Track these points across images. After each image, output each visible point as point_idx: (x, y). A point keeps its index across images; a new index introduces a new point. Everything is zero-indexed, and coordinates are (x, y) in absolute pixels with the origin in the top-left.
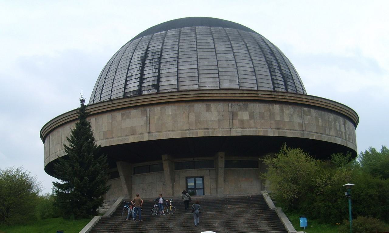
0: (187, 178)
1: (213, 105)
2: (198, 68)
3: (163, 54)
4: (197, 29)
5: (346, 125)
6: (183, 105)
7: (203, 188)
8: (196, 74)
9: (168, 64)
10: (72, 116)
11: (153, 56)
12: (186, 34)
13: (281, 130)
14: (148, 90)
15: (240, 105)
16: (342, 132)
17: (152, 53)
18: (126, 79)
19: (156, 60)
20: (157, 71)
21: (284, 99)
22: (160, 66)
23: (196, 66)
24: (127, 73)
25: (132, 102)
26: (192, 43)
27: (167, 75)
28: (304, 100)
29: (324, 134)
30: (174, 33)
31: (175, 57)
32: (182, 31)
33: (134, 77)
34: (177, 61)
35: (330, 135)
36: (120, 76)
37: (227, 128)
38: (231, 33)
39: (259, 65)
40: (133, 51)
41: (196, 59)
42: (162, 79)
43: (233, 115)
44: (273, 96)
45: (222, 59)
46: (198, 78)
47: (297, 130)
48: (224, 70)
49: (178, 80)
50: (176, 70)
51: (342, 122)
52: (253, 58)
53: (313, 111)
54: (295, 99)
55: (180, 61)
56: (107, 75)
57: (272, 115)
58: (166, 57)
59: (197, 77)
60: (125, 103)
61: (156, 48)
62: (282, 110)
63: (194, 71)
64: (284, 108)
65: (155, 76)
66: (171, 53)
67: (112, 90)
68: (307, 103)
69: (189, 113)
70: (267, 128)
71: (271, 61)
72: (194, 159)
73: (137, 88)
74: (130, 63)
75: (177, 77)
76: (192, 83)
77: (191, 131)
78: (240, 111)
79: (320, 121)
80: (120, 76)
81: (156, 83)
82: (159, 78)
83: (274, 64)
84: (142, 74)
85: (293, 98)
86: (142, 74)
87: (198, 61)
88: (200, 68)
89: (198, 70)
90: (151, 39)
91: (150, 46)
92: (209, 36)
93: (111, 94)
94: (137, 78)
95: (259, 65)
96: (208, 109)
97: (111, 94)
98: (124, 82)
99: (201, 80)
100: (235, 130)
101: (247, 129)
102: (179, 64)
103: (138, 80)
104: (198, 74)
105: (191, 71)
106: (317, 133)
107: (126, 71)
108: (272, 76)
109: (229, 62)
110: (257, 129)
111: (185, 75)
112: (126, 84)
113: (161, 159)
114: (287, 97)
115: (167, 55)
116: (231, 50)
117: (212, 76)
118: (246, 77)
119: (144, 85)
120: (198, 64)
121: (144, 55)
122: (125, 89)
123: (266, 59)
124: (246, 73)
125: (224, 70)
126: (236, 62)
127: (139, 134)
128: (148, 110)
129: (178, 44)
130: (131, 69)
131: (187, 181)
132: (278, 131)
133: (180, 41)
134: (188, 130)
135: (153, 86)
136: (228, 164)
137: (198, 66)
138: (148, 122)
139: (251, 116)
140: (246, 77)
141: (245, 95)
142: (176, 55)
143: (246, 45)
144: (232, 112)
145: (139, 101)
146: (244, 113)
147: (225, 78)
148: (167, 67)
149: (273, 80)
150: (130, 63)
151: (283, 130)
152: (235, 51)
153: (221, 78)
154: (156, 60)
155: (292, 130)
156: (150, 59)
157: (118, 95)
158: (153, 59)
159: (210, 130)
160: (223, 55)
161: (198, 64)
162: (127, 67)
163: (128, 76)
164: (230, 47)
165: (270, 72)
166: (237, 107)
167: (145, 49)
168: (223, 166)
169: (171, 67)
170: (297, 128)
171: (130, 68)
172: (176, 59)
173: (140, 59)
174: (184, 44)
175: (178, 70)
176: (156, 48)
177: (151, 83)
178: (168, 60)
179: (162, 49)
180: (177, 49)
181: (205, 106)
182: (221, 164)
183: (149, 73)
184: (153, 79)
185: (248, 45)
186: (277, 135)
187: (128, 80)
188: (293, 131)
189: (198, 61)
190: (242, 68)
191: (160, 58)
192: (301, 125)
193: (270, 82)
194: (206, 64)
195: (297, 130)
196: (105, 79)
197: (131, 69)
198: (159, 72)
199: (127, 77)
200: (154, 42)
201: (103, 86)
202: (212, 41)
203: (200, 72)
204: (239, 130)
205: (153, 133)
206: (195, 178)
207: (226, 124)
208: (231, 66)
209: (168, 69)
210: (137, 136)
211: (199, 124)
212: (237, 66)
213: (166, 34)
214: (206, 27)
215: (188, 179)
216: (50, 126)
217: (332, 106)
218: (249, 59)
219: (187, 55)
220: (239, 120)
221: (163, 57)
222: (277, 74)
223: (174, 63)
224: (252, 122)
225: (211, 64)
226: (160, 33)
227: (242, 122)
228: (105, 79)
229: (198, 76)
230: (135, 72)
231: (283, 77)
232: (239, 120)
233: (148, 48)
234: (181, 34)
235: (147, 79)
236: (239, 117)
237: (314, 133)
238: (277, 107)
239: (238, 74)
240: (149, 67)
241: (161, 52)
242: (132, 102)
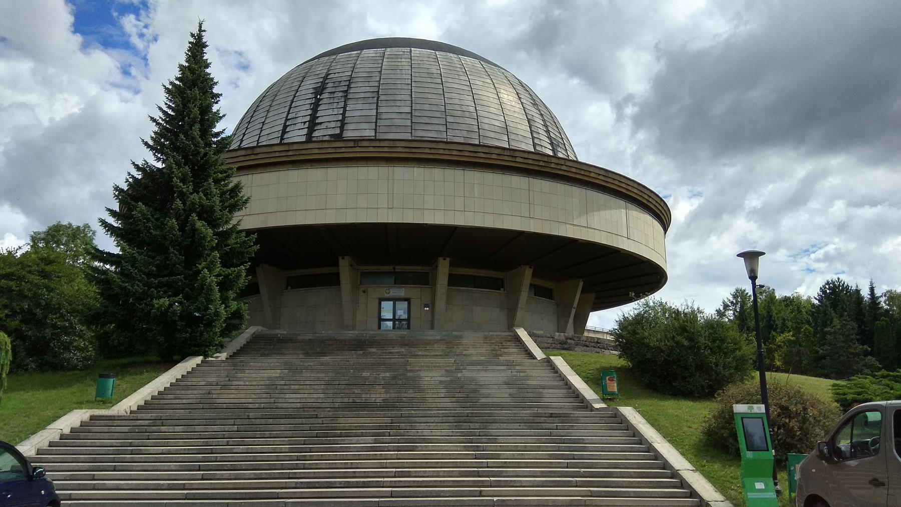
0: (381, 300)
8: (409, 123)
18: (285, 123)
19: (341, 94)
21: (560, 169)
22: (346, 105)
24: (288, 113)
33: (300, 120)
40: (301, 79)
42: (346, 127)
49: (375, 130)
55: (382, 98)
56: (252, 117)
60: (277, 154)
61: (341, 75)
63: (404, 116)
68: (597, 181)
73: (303, 139)
81: (338, 131)
82: (343, 124)
84: (314, 117)
85: (574, 170)
86: (314, 117)
94: (305, 123)
98: (281, 127)
103: (307, 125)
105: (400, 116)
108: (533, 138)
109: (464, 108)
112: (284, 132)
113: (336, 264)
114: (564, 168)
119: (315, 134)
129: (380, 72)
131: (380, 304)
136: (454, 280)
140: (492, 135)
141: (494, 156)
145: (303, 152)
154: (341, 94)
168: (446, 283)
172: (375, 95)
173: (312, 91)
176: (341, 75)
183: (328, 115)
196: (249, 122)
199: (287, 120)
201: (244, 135)
223: (370, 100)
228: (249, 122)
230: (303, 112)
231: (552, 144)
242: (291, 153)
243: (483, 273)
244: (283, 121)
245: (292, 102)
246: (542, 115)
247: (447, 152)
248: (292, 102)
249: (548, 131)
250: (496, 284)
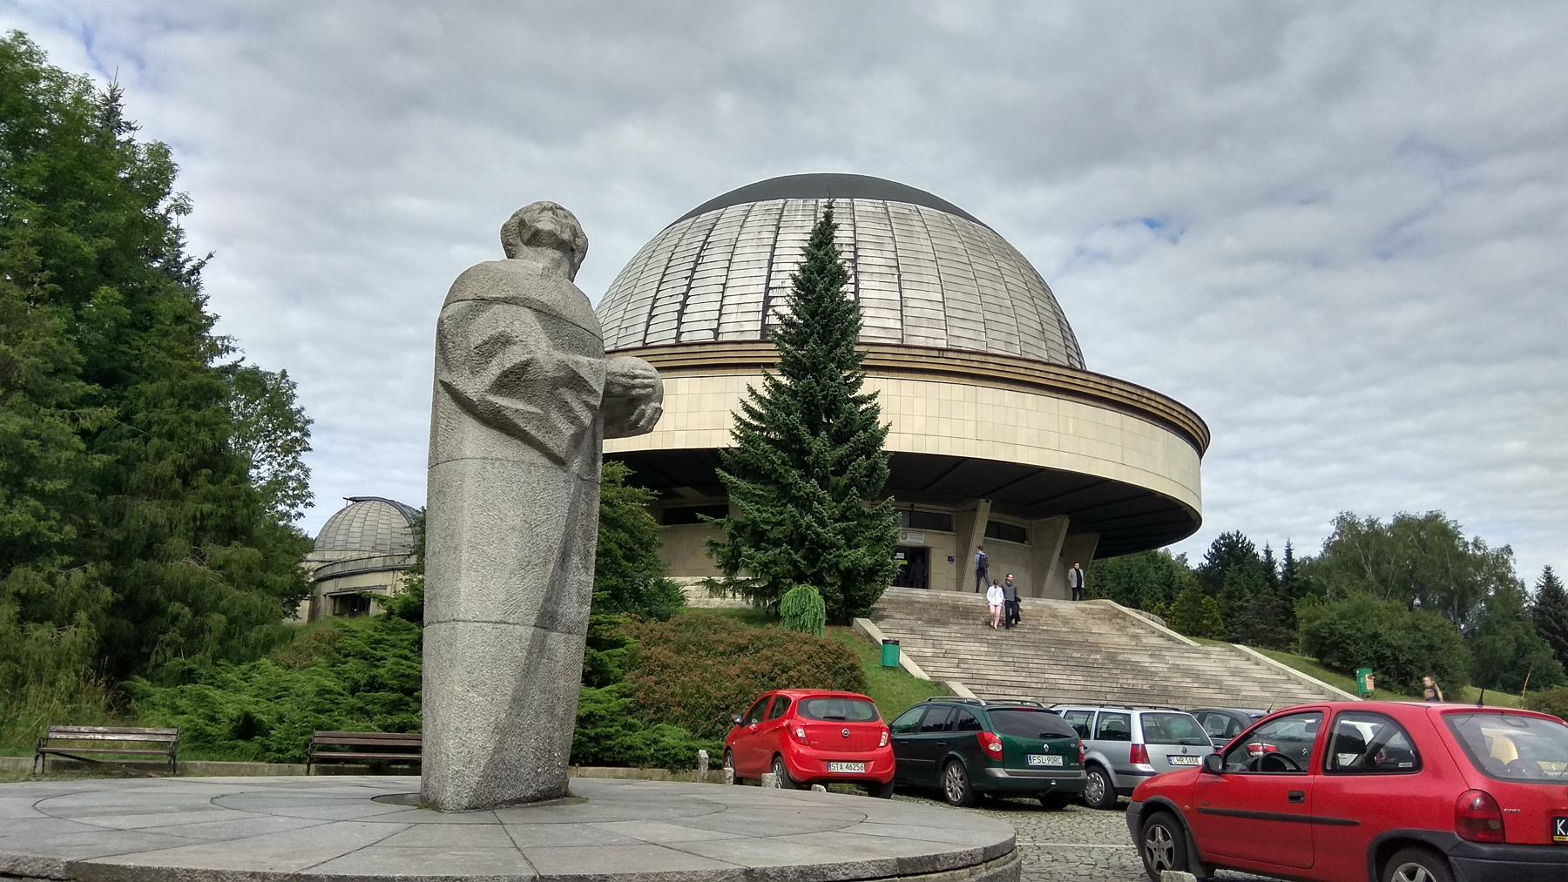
18: (766, 293)
24: (769, 279)
58: (869, 260)
98: (761, 298)
105: (928, 305)
107: (765, 272)
109: (1001, 302)
136: (994, 530)
150: (772, 255)
160: (988, 283)
171: (774, 268)
178: (876, 269)
182: (980, 528)
194: (959, 296)
199: (768, 289)
223: (889, 278)
244: (762, 288)
245: (771, 263)
248: (771, 263)
250: (1020, 536)
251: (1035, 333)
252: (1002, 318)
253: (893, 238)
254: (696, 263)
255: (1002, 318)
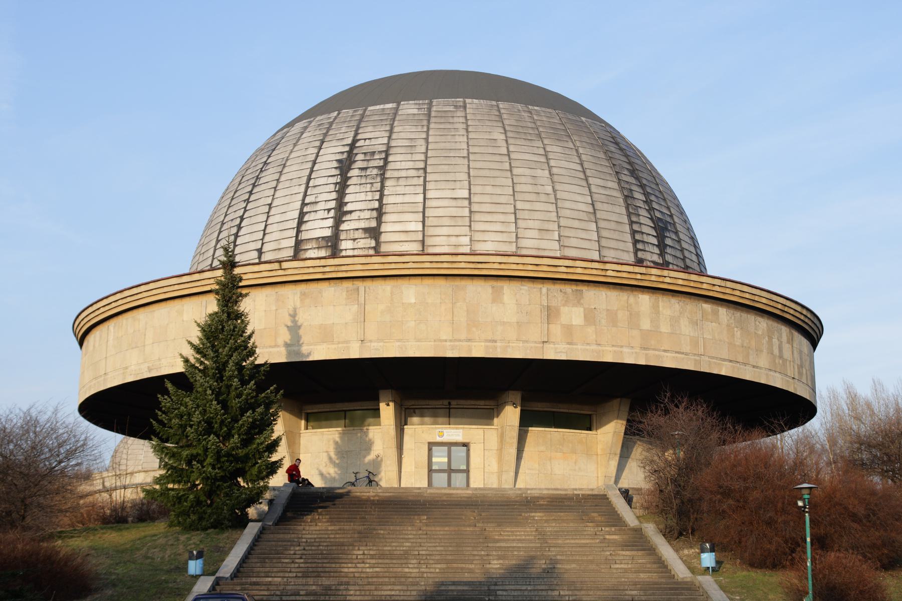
1: (508, 288)
2: (470, 199)
3: (390, 159)
4: (468, 106)
5: (795, 345)
6: (441, 282)
7: (467, 471)
8: (466, 212)
9: (402, 182)
10: (177, 287)
11: (368, 160)
12: (443, 115)
13: (651, 352)
14: (354, 240)
15: (565, 293)
16: (785, 361)
17: (365, 154)
18: (302, 209)
19: (375, 171)
20: (377, 197)
23: (465, 194)
24: (305, 195)
25: (327, 269)
26: (458, 139)
27: (400, 208)
28: (705, 286)
29: (745, 364)
30: (416, 111)
31: (418, 169)
32: (434, 109)
33: (321, 206)
34: (422, 179)
35: (757, 367)
36: (287, 200)
37: (536, 342)
38: (544, 119)
39: (603, 198)
40: (318, 144)
41: (465, 177)
42: (385, 218)
43: (550, 314)
44: (639, 277)
45: (523, 180)
46: (471, 221)
47: (686, 354)
48: (527, 206)
49: (423, 222)
50: (420, 198)
51: (784, 338)
52: (591, 180)
53: (723, 311)
54: (685, 283)
57: (634, 318)
58: (398, 166)
59: (467, 219)
60: (311, 270)
62: (655, 308)
64: (661, 304)
65: (373, 210)
66: (409, 157)
67: (264, 230)
69: (453, 304)
70: (622, 347)
71: (631, 190)
72: (450, 404)
73: (328, 233)
74: (312, 171)
75: (421, 215)
76: (457, 231)
77: (457, 343)
78: (564, 305)
79: (738, 333)
80: (287, 200)
81: (374, 224)
82: (380, 212)
83: (636, 195)
84: (340, 202)
85: (680, 282)
86: (340, 202)
87: (470, 182)
88: (474, 199)
89: (470, 203)
90: (360, 121)
91: (359, 137)
92: (495, 124)
93: (262, 239)
94: (329, 210)
95: (603, 198)
96: (497, 298)
97: (262, 239)
98: (296, 214)
99: (476, 226)
100: (552, 346)
101: (579, 347)
102: (428, 186)
103: (332, 213)
104: (471, 212)
105: (453, 203)
106: (731, 361)
107: (303, 187)
109: (540, 189)
110: (600, 348)
111: (440, 212)
112: (301, 222)
114: (667, 280)
115: (398, 161)
116: (543, 159)
117: (501, 218)
118: (576, 224)
119: (344, 227)
120: (470, 190)
121: (345, 156)
122: (299, 231)
123: (619, 184)
124: (575, 215)
125: (527, 206)
126: (555, 191)
127: (339, 343)
128: (362, 290)
129: (427, 140)
130: (315, 187)
132: (646, 355)
133: (431, 133)
134: (451, 341)
135: (366, 230)
137: (470, 194)
138: (363, 318)
139: (590, 317)
140: (576, 224)
141: (579, 271)
142: (422, 165)
143: (577, 151)
144: (549, 308)
145: (344, 268)
146: (574, 309)
147: (530, 224)
148: (401, 190)
149: (634, 233)
150: (312, 171)
151: (657, 353)
152: (552, 163)
153: (521, 224)
155: (676, 352)
156: (359, 168)
157: (279, 244)
158: (365, 169)
159: (498, 344)
160: (527, 172)
161: (470, 190)
162: (304, 180)
163: (306, 202)
164: (542, 151)
165: (629, 215)
166: (560, 297)
167: (349, 141)
169: (408, 190)
170: (687, 348)
171: (311, 184)
172: (421, 172)
173: (335, 164)
174: (438, 139)
175: (425, 199)
176: (373, 142)
177: (363, 224)
178: (403, 174)
179: (389, 147)
180: (423, 150)
181: (490, 290)
183: (359, 198)
184: (367, 214)
185: (581, 151)
186: (642, 362)
187: (307, 213)
188: (677, 355)
189: (470, 182)
190: (567, 204)
191: (383, 169)
192: (695, 342)
193: (628, 238)
194: (489, 189)
195: (686, 354)
196: (247, 201)
197: (315, 187)
198: (380, 200)
199: (304, 204)
200: (370, 129)
201: (242, 218)
202: (503, 137)
203: (475, 208)
204: (563, 347)
205: (371, 341)
206: (450, 445)
207: (535, 333)
208: (543, 198)
209: (401, 195)
210: (334, 346)
211: (474, 329)
212: (556, 199)
213: (397, 109)
214: (489, 102)
215: (434, 448)
216: (114, 305)
217: (764, 301)
218: (584, 183)
219: (447, 167)
220: (563, 326)
221: (390, 166)
222: (643, 220)
223: (415, 181)
224: (590, 330)
225: (498, 191)
226: (382, 106)
227: (569, 330)
228: (247, 201)
229: (470, 217)
230: (325, 196)
232: (563, 326)
233: (355, 141)
234: (433, 114)
235: (353, 214)
236: (564, 319)
237: (724, 360)
238: (645, 299)
239: (558, 217)
240: (358, 187)
241: (387, 153)
242: (327, 269)
243: (563, 409)
245: (309, 179)
246: (642, 186)
247: (520, 267)
248: (309, 179)
249: (651, 210)
251: (584, 216)
252: (538, 206)
253: (427, 140)
254: (254, 186)
255: (538, 206)
